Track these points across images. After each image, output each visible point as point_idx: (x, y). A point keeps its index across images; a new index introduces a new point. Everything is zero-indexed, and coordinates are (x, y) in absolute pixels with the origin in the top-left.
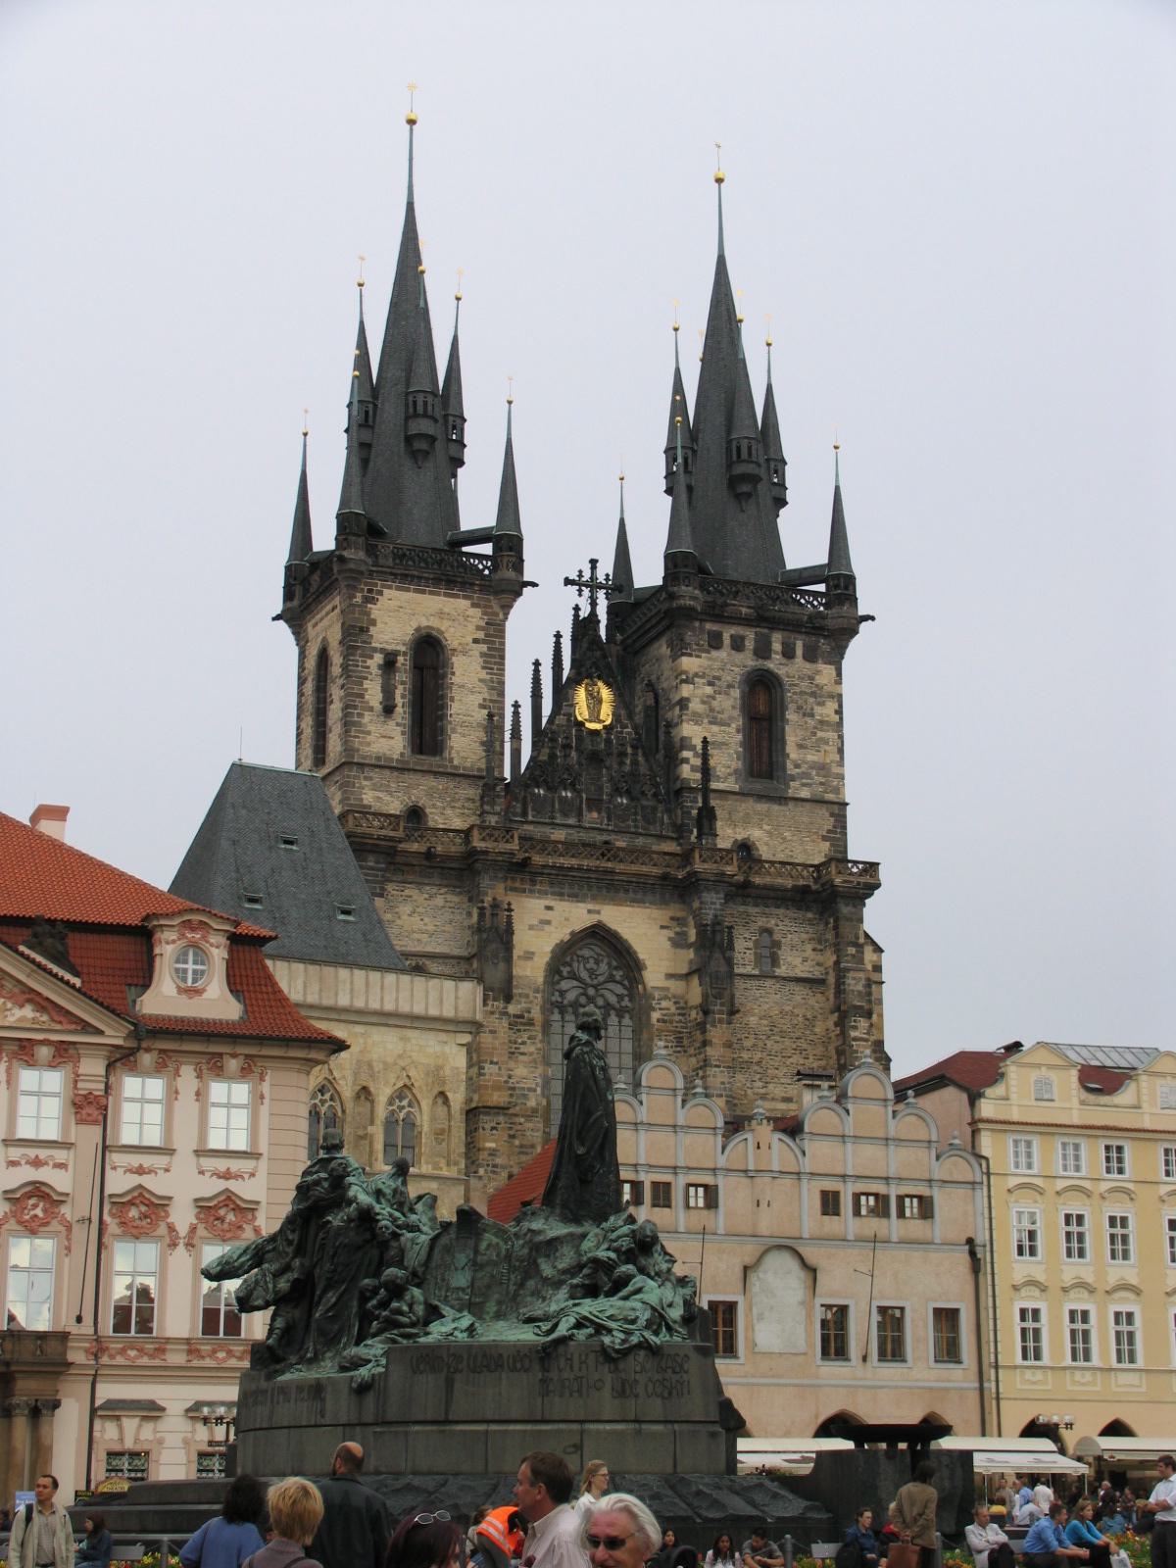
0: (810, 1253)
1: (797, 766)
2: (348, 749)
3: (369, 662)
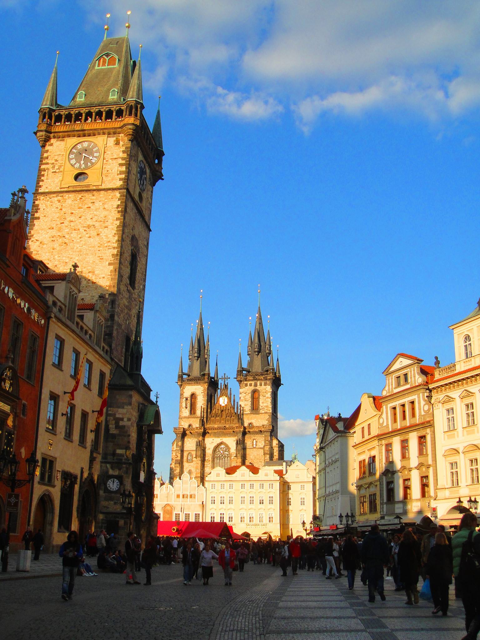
1: (262, 407)
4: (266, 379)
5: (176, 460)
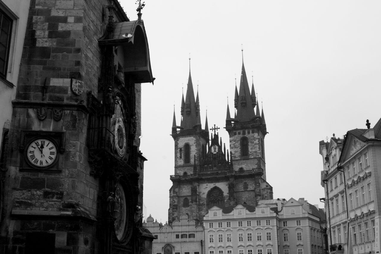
0: (174, 245)
1: (251, 152)
2: (175, 165)
3: (178, 150)
4: (253, 128)
5: (174, 205)
